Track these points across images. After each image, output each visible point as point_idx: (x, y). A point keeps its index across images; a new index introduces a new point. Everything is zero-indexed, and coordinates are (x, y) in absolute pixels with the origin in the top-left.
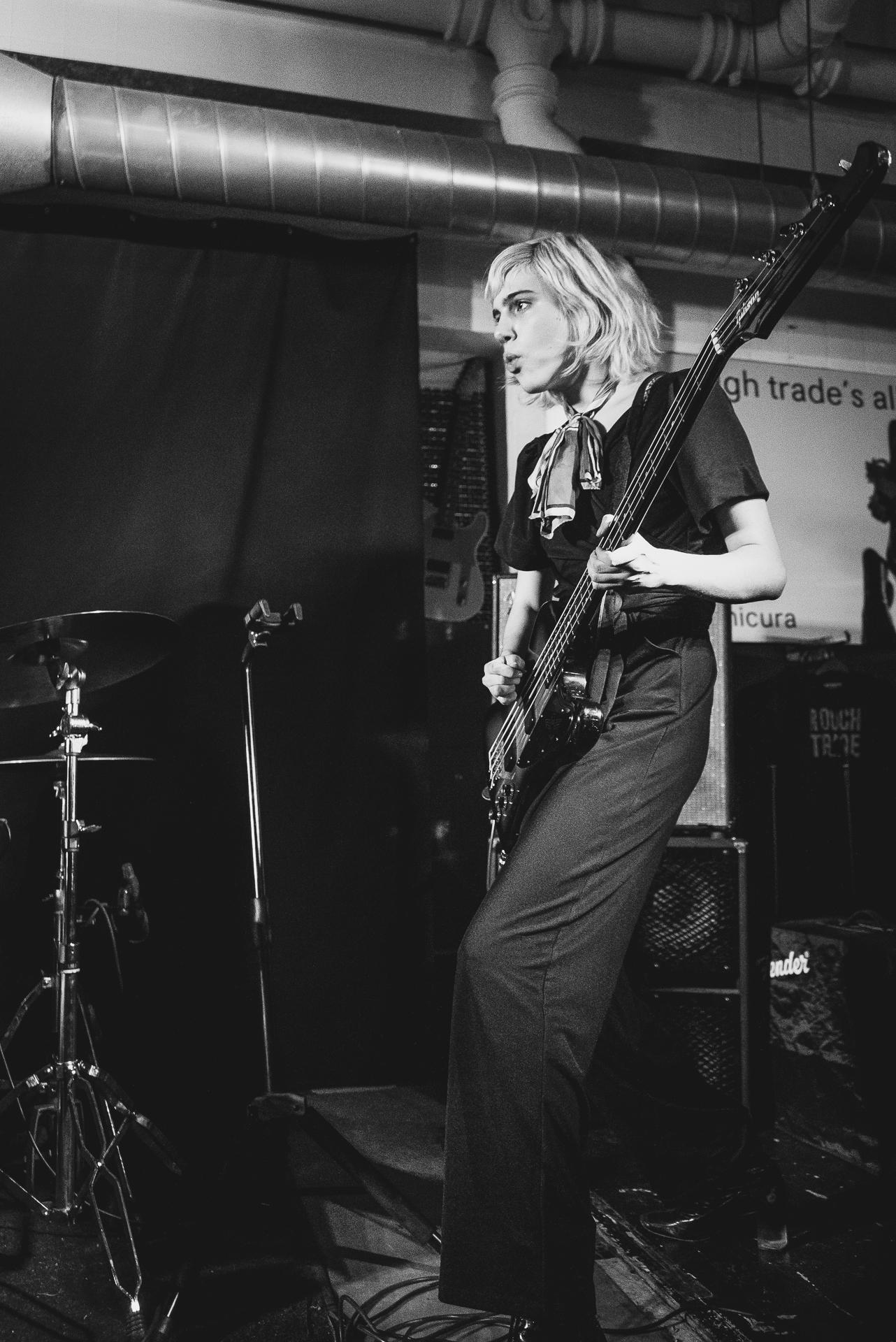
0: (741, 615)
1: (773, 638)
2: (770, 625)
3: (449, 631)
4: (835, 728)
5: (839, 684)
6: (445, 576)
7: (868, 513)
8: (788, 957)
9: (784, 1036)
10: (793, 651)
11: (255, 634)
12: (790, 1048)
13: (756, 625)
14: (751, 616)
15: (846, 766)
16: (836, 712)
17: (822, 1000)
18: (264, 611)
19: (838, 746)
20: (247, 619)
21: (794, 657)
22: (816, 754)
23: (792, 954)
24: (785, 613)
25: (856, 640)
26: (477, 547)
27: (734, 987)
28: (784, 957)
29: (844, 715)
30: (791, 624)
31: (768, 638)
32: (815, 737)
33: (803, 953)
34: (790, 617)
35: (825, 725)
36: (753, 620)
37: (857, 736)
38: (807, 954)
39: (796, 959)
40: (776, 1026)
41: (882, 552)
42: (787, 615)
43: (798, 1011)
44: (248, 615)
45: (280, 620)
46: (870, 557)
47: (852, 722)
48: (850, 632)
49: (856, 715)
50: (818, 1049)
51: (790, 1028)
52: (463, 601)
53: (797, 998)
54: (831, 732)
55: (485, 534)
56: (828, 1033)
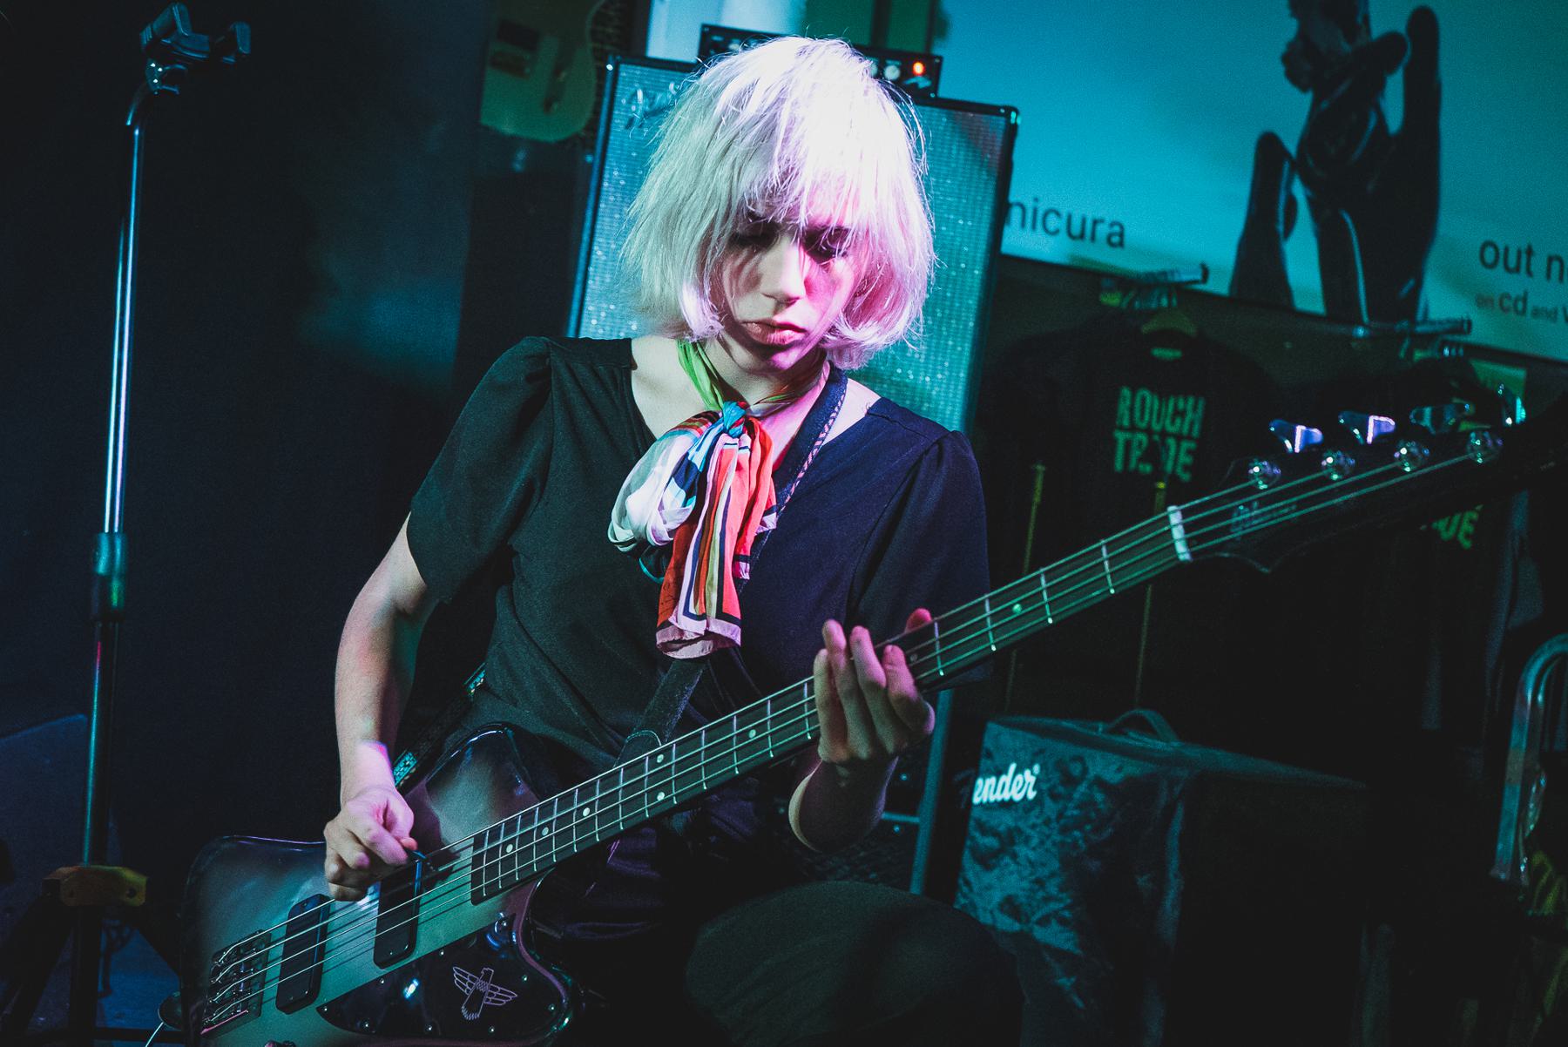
0: (1035, 211)
1: (1083, 260)
2: (1082, 236)
3: (521, 155)
4: (1156, 427)
5: (1178, 354)
6: (528, 56)
7: (1280, 69)
8: (1006, 772)
9: (977, 899)
10: (1111, 290)
11: (157, 67)
12: (985, 918)
13: (1056, 232)
14: (1052, 217)
15: (1162, 485)
16: (1163, 396)
17: (1048, 844)
18: (179, 24)
19: (1154, 453)
20: (146, 36)
21: (1112, 300)
22: (1119, 466)
23: (1013, 767)
24: (1108, 220)
25: (1219, 285)
26: (593, 12)
27: (913, 812)
28: (999, 772)
29: (1176, 406)
30: (1117, 240)
31: (1074, 258)
32: (1121, 437)
33: (1031, 767)
34: (1117, 229)
36: (1053, 223)
37: (1193, 445)
38: (1037, 768)
39: (1019, 777)
40: (967, 883)
41: (1292, 146)
42: (1112, 224)
43: (1007, 860)
44: (149, 29)
45: (207, 48)
46: (1269, 147)
49: (1195, 408)
50: (1028, 921)
51: (989, 887)
52: (555, 106)
53: (1009, 841)
54: (1149, 431)
56: (1048, 899)
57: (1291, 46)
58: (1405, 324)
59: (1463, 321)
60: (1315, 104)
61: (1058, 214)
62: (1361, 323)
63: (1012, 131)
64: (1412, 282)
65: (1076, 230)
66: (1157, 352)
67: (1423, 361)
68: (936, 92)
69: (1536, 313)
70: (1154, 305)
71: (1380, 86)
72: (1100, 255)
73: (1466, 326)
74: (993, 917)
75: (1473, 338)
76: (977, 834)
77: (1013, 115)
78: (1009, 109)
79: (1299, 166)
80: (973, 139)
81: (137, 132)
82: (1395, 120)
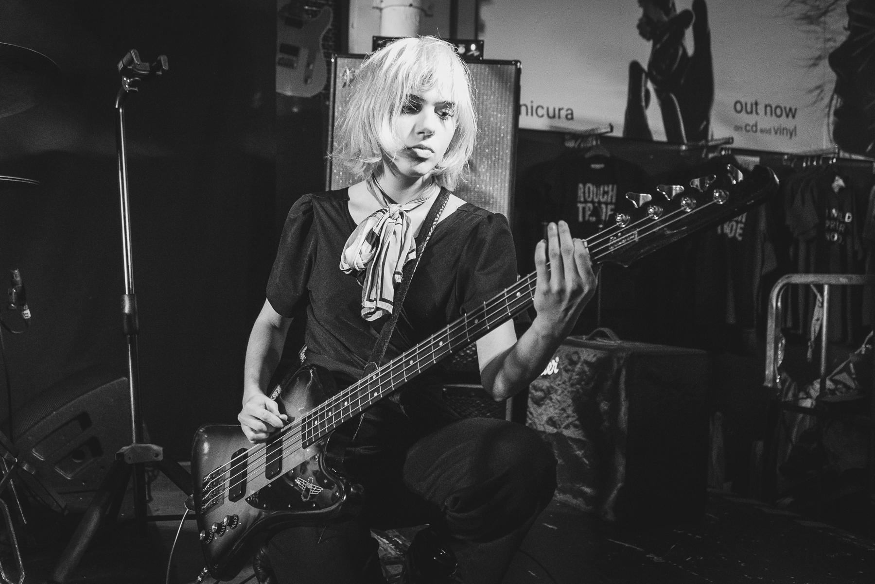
0: (532, 107)
1: (556, 127)
2: (554, 117)
4: (596, 200)
5: (602, 166)
6: (294, 59)
7: (637, 32)
9: (536, 421)
10: (570, 140)
13: (542, 116)
16: (598, 187)
17: (566, 392)
18: (135, 59)
19: (596, 212)
20: (121, 66)
21: (570, 144)
22: (581, 219)
24: (566, 108)
25: (618, 133)
26: (322, 36)
29: (604, 189)
30: (570, 117)
31: (551, 127)
32: (580, 206)
33: (554, 359)
34: (569, 112)
35: (589, 196)
36: (540, 112)
40: (531, 413)
41: (645, 66)
42: (567, 110)
43: (548, 401)
46: (635, 67)
47: (610, 195)
48: (613, 124)
49: (612, 190)
50: (560, 427)
51: (541, 414)
54: (592, 202)
55: (329, 26)
56: (568, 417)
57: (641, 20)
58: (703, 142)
59: (729, 139)
60: (654, 45)
61: (542, 108)
62: (683, 144)
63: (518, 72)
64: (705, 123)
65: (551, 114)
66: (593, 166)
67: (713, 158)
68: (482, 56)
69: (762, 131)
70: (590, 145)
71: (682, 35)
72: (563, 124)
73: (731, 141)
74: (544, 427)
75: (736, 145)
76: (533, 391)
77: (518, 64)
78: (517, 62)
79: (649, 75)
80: (501, 77)
81: (121, 111)
82: (690, 51)
